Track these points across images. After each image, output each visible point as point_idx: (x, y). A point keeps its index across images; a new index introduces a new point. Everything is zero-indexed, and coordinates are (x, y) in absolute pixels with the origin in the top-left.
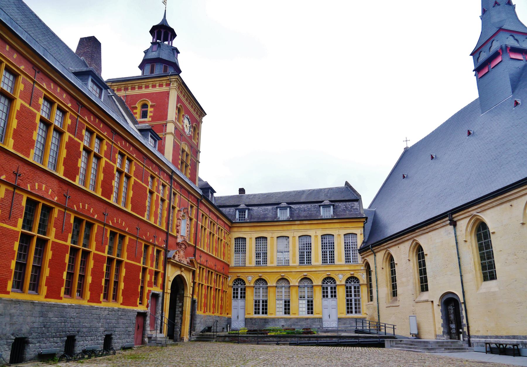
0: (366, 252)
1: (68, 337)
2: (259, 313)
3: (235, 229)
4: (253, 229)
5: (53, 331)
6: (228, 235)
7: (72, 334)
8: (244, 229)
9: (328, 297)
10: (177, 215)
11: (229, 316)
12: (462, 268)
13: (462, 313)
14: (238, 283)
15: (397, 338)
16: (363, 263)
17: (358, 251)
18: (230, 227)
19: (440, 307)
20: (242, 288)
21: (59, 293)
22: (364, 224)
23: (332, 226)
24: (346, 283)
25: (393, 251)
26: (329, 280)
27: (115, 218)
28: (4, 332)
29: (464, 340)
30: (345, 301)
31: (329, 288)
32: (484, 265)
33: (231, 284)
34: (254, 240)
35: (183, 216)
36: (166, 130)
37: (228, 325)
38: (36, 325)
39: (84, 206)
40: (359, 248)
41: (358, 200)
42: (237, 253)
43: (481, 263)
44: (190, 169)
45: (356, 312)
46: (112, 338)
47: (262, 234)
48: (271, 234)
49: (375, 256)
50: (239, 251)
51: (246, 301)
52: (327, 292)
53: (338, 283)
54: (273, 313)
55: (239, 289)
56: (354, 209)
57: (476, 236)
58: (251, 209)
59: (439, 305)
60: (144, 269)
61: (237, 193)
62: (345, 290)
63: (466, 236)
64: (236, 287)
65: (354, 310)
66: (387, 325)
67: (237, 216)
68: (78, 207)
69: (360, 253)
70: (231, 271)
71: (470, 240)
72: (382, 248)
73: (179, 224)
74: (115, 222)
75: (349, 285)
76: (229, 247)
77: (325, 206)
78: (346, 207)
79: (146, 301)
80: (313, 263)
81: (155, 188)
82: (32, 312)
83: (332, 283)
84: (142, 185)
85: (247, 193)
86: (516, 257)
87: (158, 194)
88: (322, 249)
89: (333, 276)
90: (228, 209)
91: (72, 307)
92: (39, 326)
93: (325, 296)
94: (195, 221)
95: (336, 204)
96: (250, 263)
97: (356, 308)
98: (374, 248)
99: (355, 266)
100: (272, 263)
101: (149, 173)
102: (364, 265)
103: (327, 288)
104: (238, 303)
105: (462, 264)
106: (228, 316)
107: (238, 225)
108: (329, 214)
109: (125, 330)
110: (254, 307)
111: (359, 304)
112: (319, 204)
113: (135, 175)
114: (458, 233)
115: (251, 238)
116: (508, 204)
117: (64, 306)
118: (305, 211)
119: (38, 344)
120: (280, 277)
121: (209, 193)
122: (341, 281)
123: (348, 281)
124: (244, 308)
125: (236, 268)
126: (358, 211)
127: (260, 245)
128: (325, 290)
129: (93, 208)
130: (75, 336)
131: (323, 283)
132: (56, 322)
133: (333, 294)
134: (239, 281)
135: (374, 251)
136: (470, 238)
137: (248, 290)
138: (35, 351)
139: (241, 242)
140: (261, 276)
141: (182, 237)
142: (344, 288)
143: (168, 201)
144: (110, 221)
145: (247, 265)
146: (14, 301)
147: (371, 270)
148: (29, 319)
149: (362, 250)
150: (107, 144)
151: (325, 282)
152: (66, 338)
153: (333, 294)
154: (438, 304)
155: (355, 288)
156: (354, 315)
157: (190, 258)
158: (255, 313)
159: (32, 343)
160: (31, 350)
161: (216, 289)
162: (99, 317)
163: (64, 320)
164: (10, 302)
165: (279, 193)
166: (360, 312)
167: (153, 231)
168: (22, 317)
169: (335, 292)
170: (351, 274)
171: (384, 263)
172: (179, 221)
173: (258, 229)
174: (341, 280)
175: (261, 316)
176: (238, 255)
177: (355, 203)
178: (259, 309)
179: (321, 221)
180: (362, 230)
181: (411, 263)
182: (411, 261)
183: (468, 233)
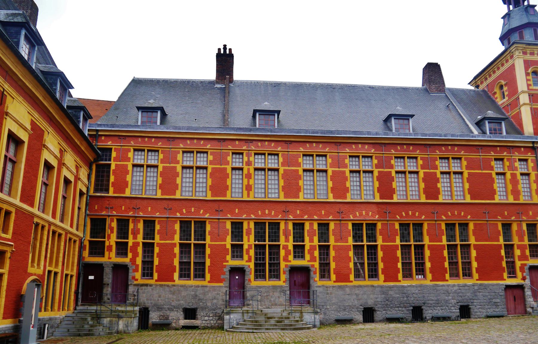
1: (413, 307)
5: (397, 303)
7: (417, 305)
21: (397, 278)
28: (354, 304)
36: (519, 103)
38: (379, 300)
39: (407, 214)
46: (470, 308)
60: (509, 248)
68: (401, 216)
79: (519, 274)
81: (506, 168)
82: (373, 292)
84: (483, 173)
87: (515, 172)
91: (412, 286)
101: (492, 158)
109: (489, 302)
113: (467, 168)
117: (403, 286)
129: (418, 212)
130: (421, 306)
132: (398, 297)
138: (382, 316)
146: (357, 286)
148: (372, 296)
150: (421, 159)
152: (412, 308)
159: (378, 311)
160: (378, 315)
162: (448, 292)
163: (406, 295)
164: (354, 287)
168: (366, 295)
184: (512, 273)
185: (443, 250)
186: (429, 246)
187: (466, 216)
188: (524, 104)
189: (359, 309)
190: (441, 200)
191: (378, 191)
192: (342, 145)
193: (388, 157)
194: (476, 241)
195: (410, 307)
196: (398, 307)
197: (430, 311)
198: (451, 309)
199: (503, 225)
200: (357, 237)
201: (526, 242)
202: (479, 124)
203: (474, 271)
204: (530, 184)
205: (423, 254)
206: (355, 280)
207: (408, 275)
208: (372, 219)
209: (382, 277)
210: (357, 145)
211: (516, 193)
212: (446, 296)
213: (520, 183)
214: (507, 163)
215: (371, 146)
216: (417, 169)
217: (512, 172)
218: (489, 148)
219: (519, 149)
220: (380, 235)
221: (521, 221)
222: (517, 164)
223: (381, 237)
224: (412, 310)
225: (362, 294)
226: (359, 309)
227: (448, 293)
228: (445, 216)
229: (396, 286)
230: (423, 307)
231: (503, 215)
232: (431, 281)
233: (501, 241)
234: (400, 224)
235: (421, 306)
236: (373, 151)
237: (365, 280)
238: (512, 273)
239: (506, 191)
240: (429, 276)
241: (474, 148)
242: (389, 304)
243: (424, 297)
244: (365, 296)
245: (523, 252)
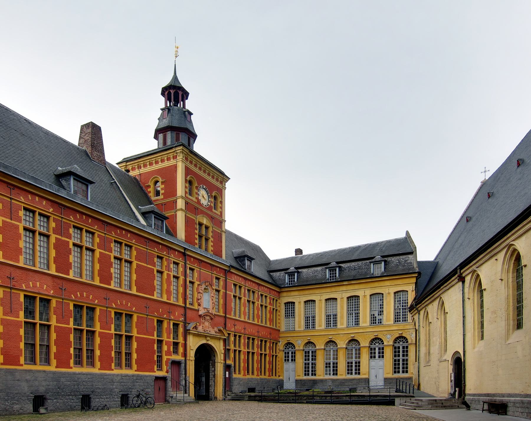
2: (308, 375)
3: (285, 294)
4: (302, 293)
6: (276, 300)
8: (293, 293)
10: (197, 289)
11: (281, 378)
14: (289, 347)
18: (279, 293)
20: (292, 351)
23: (382, 284)
27: (118, 301)
31: (377, 349)
33: (282, 348)
34: (303, 304)
35: (205, 289)
37: (279, 387)
42: (288, 318)
44: (212, 241)
47: (310, 297)
48: (319, 297)
50: (289, 316)
51: (296, 364)
52: (375, 353)
54: (321, 374)
55: (290, 353)
58: (301, 271)
61: (293, 254)
64: (287, 351)
65: (401, 370)
67: (287, 281)
69: (410, 311)
70: (281, 335)
73: (200, 298)
74: (119, 304)
76: (279, 312)
78: (399, 262)
80: (361, 324)
85: (304, 253)
87: (170, 273)
89: (380, 336)
90: (278, 274)
92: (54, 388)
93: (372, 357)
94: (223, 292)
95: (389, 259)
96: (299, 327)
98: (418, 306)
99: (404, 325)
100: (320, 326)
104: (289, 366)
106: (280, 378)
107: (286, 290)
110: (304, 369)
112: (370, 261)
115: (300, 302)
118: (355, 270)
119: (55, 400)
120: (328, 340)
121: (245, 261)
123: (397, 341)
124: (295, 370)
125: (285, 333)
127: (309, 309)
128: (373, 351)
131: (371, 344)
134: (289, 344)
137: (297, 353)
139: (290, 307)
140: (310, 340)
141: (205, 309)
143: (184, 278)
144: (113, 304)
145: (297, 329)
148: (44, 383)
151: (373, 342)
153: (381, 355)
156: (401, 375)
157: (219, 327)
158: (305, 375)
159: (50, 399)
161: (261, 354)
165: (335, 251)
167: (166, 307)
172: (199, 294)
173: (307, 292)
174: (388, 341)
175: (310, 377)
176: (287, 320)
178: (308, 371)
179: (370, 279)
184: (160, 368)
185: (111, 339)
186: (100, 333)
187: (131, 307)
188: (182, 210)
189: (29, 397)
190: (112, 287)
191: (55, 262)
192: (16, 191)
193: (67, 223)
194: (138, 333)
195: (80, 395)
196: (69, 396)
197: (97, 400)
198: (114, 398)
199: (158, 321)
200: (29, 313)
201: (171, 340)
202: (144, 214)
203: (134, 362)
204: (177, 287)
205: (93, 340)
206: (25, 364)
207: (79, 362)
208: (47, 293)
209: (54, 362)
210: (34, 196)
211: (169, 292)
212: (111, 385)
213: (172, 285)
214: (165, 263)
215: (50, 203)
216: (93, 246)
217: (168, 272)
218: (154, 244)
219: (174, 251)
220: (54, 314)
221: (170, 320)
222: (172, 266)
223: (55, 316)
224: (82, 399)
225: (34, 381)
226: (29, 397)
227: (112, 381)
228: (115, 304)
229: (68, 373)
230: (91, 396)
231: (158, 312)
232: (99, 369)
233: (155, 337)
234: (74, 305)
235: (90, 395)
236: (51, 210)
237: (36, 365)
238: (160, 368)
239: (161, 290)
240: (98, 364)
241: (143, 240)
242: (60, 392)
243: (92, 385)
244: (37, 383)
245: (169, 348)
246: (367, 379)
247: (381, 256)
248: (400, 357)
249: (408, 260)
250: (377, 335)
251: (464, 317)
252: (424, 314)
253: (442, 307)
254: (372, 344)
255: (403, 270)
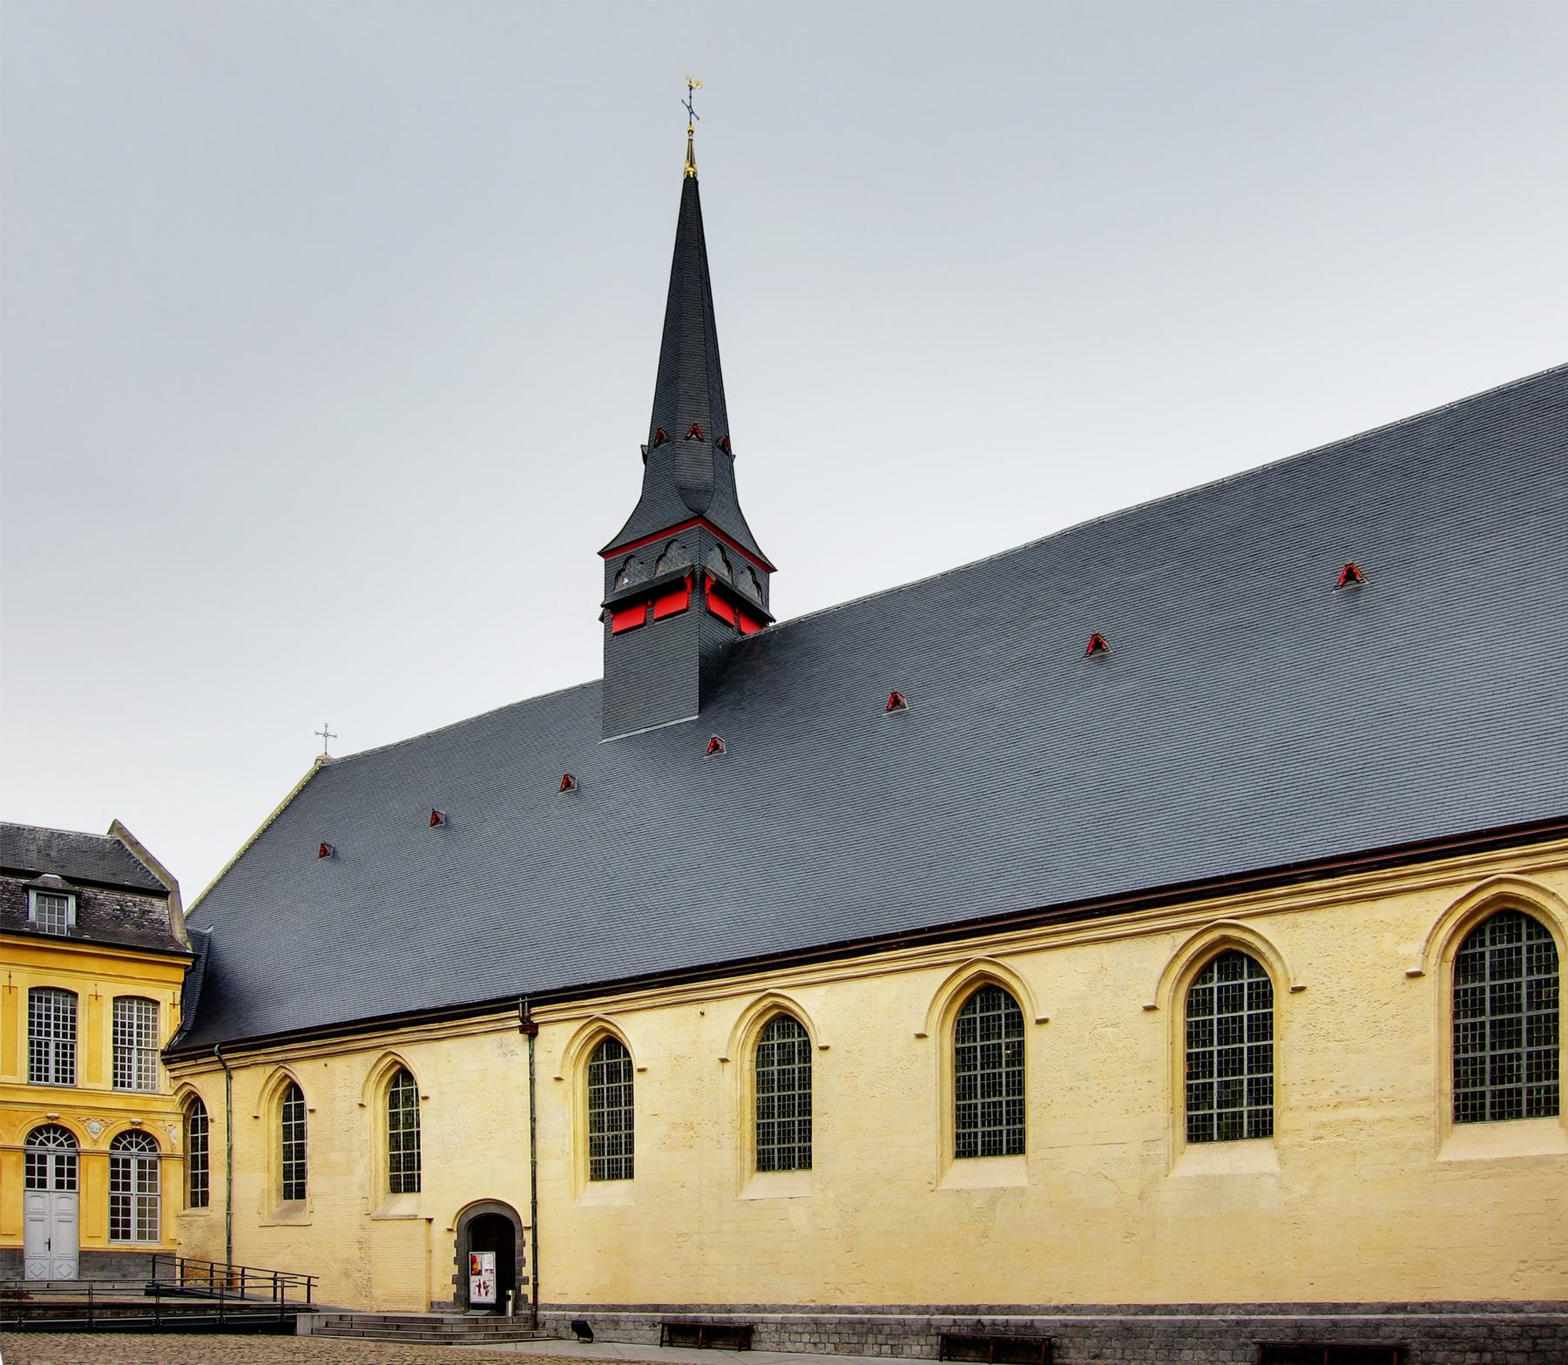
0: (193, 1062)
9: (45, 1187)
12: (539, 1144)
13: (521, 1252)
15: (318, 1311)
16: (175, 1093)
17: (158, 1055)
19: (454, 1236)
22: (186, 974)
24: (113, 1147)
25: (307, 1074)
26: (52, 1135)
29: (514, 1314)
30: (107, 1200)
32: (597, 1142)
40: (162, 1046)
41: (168, 893)
43: (591, 1138)
45: (141, 1236)
49: (230, 1078)
53: (84, 1145)
56: (152, 921)
57: (588, 1071)
59: (450, 1230)
62: (108, 1169)
63: (562, 1066)
65: (134, 1229)
66: (247, 1272)
69: (166, 1062)
71: (572, 1078)
72: (261, 1059)
75: (120, 1154)
77: (46, 892)
78: (122, 910)
83: (61, 1144)
86: (692, 1133)
88: (31, 1032)
97: (141, 1224)
99: (148, 1099)
102: (178, 1099)
103: (43, 1159)
105: (538, 1135)
108: (61, 921)
111: (153, 1213)
114: (538, 1057)
116: (696, 1008)
122: (95, 1142)
123: (121, 1143)
126: (163, 930)
133: (66, 1178)
135: (228, 1064)
136: (572, 1073)
142: (107, 1161)
147: (209, 1116)
149: (172, 1056)
154: (450, 1227)
155: (141, 1164)
166: (153, 1236)
169: (72, 1173)
170: (133, 1123)
171: (264, 1104)
177: (155, 901)
180: (179, 993)
181: (368, 1115)
182: (370, 1108)
183: (570, 1061)
246: (17, 1252)
247: (63, 877)
248: (129, 1190)
249: (150, 911)
250: (140, 1124)
251: (533, 1120)
252: (267, 1082)
253: (381, 1077)
254: (34, 1144)
255: (142, 937)
